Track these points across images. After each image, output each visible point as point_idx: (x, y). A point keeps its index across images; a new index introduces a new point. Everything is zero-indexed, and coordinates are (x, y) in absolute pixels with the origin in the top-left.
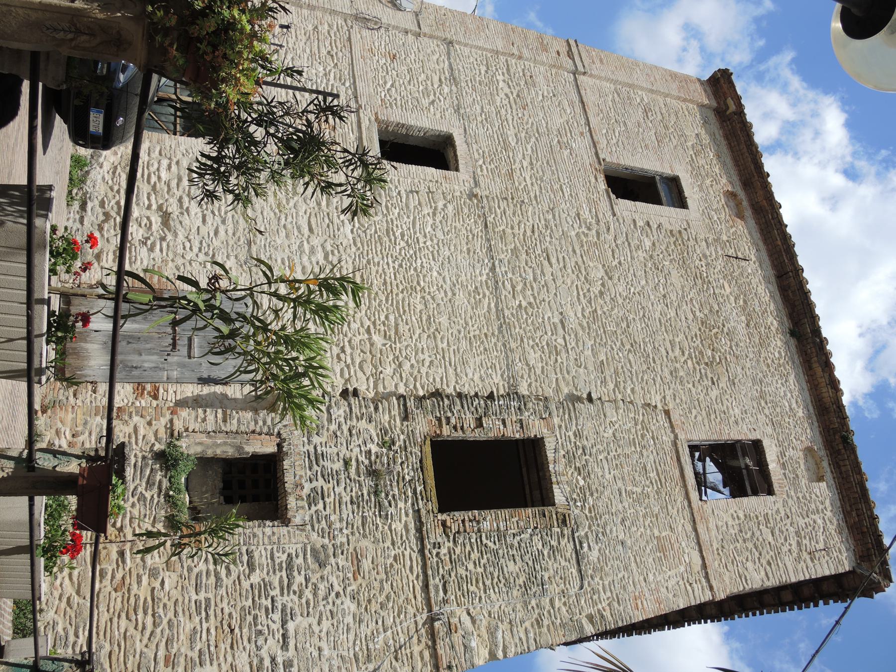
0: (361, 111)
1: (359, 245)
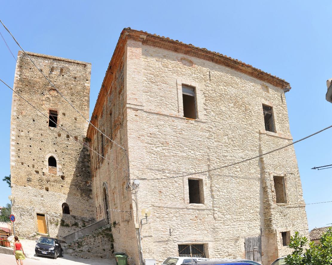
1: (231, 214)
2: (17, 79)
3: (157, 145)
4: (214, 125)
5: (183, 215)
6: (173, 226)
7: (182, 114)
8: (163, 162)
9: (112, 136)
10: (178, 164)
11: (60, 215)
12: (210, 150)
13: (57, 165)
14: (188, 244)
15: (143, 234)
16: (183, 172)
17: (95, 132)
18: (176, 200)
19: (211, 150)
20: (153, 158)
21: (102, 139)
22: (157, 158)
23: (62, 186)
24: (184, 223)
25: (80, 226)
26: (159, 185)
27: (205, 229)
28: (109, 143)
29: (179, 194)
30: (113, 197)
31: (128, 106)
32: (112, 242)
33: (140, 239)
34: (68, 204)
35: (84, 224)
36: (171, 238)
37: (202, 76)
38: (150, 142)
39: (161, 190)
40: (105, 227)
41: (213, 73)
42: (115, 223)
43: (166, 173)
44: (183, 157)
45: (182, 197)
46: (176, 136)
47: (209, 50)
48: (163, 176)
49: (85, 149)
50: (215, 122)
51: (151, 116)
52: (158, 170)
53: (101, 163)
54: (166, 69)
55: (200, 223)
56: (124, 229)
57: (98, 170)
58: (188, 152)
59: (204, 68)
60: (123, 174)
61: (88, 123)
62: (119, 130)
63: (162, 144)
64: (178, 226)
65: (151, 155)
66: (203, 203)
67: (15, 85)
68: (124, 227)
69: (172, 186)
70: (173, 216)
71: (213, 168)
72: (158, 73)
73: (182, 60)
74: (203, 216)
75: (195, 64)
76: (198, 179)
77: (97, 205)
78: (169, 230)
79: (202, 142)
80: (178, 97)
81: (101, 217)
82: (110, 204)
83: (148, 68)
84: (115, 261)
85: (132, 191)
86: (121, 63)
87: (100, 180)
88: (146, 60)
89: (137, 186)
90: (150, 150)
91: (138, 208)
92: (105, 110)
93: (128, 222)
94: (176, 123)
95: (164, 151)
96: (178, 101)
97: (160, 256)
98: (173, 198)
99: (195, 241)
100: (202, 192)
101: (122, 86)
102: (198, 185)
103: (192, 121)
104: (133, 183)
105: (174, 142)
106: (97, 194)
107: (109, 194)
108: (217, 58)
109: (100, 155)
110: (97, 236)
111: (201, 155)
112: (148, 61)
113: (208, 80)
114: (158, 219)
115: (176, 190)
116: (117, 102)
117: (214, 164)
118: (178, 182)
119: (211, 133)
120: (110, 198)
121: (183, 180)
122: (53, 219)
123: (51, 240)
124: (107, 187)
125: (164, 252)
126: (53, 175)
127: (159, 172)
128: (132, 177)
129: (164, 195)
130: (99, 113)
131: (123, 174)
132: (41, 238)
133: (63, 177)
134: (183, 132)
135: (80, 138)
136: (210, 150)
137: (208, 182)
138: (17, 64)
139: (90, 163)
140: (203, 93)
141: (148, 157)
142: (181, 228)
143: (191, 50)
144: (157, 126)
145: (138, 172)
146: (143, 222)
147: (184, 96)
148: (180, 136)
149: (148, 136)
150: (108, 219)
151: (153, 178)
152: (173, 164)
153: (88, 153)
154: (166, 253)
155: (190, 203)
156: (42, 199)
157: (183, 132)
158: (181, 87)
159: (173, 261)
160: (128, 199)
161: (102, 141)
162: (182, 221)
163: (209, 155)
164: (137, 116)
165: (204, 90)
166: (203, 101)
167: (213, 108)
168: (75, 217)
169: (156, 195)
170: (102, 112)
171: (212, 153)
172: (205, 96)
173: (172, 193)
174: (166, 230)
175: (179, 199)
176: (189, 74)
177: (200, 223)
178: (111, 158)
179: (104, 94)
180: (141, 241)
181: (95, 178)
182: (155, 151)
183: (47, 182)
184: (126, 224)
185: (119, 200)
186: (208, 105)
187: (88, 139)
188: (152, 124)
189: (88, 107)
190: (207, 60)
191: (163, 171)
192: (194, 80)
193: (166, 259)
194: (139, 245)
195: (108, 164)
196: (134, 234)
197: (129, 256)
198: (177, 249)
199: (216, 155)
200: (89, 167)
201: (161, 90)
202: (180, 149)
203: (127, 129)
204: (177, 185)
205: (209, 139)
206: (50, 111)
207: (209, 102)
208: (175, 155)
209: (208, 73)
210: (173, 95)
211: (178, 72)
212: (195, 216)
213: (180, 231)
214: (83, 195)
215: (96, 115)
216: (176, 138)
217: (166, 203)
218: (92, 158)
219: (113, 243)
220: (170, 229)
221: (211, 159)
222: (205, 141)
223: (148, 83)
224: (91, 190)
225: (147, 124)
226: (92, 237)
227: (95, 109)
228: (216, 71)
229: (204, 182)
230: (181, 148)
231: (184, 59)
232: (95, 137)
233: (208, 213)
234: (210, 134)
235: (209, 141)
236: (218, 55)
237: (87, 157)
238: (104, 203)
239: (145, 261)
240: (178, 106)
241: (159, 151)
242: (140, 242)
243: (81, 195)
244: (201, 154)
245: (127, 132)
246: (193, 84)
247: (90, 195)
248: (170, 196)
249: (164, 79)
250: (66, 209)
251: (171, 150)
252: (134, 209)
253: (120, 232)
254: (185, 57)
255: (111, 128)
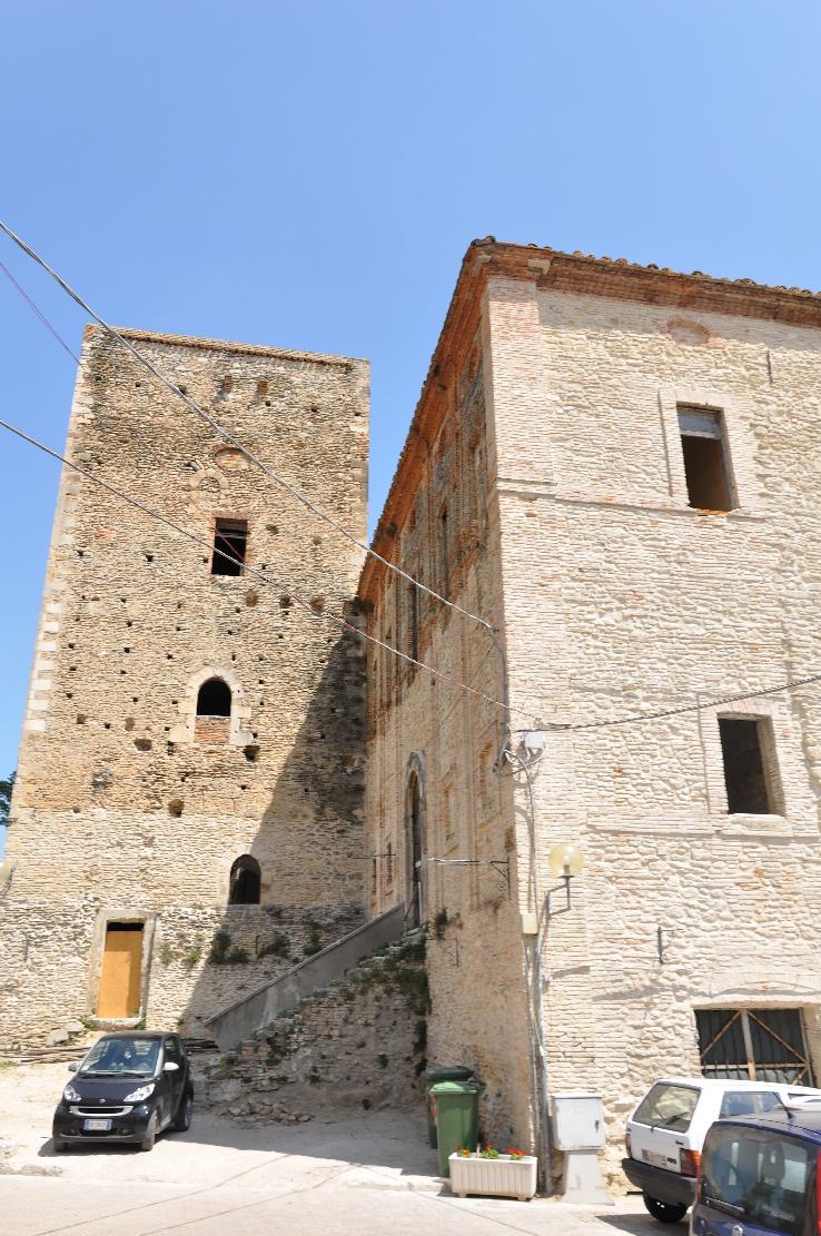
0: (724, 832)
2: (81, 420)
3: (604, 606)
4: (797, 526)
5: (708, 863)
6: (673, 917)
7: (682, 498)
8: (627, 663)
9: (447, 585)
10: (680, 664)
11: (214, 912)
12: (788, 612)
13: (234, 708)
14: (733, 1007)
15: (553, 960)
16: (699, 694)
17: (387, 579)
18: (677, 801)
19: (793, 609)
20: (591, 651)
21: (414, 600)
22: (604, 648)
23: (243, 787)
24: (712, 902)
25: (296, 951)
26: (613, 744)
27: (801, 931)
28: (438, 610)
29: (689, 777)
30: (443, 805)
31: (501, 486)
32: (422, 1013)
33: (541, 985)
34: (260, 857)
35: (315, 939)
36: (666, 974)
37: (743, 371)
38: (579, 597)
39: (621, 766)
40: (401, 944)
41: (780, 356)
42: (442, 920)
43: (636, 697)
44: (694, 639)
45: (699, 789)
46: (668, 572)
47: (760, 282)
48: (629, 712)
49: (350, 640)
50: (799, 514)
51: (582, 513)
52: (612, 692)
53: (405, 684)
54: (623, 361)
55: (778, 900)
56: (478, 943)
57: (394, 709)
58: (713, 622)
59: (747, 345)
60: (484, 713)
61: (365, 553)
62: (472, 570)
63: (622, 601)
64: (689, 916)
65: (584, 640)
66: (782, 814)
67: (70, 441)
68: (479, 932)
69: (662, 747)
70: (668, 867)
71: (805, 672)
72: (595, 376)
73: (672, 326)
74: (786, 868)
75: (717, 335)
76: (754, 719)
77: (378, 848)
78: (654, 936)
79: (757, 584)
80: (665, 447)
81: (386, 899)
82: (432, 841)
83: (561, 362)
84: (425, 1121)
85: (515, 776)
86: (473, 356)
87: (399, 745)
88: (554, 338)
89: (536, 756)
90: (583, 624)
91: (536, 844)
92: (425, 505)
93: (496, 907)
94: (664, 530)
95: (630, 624)
96: (666, 458)
97: (622, 1075)
98: (666, 791)
99: (764, 992)
100: (771, 767)
101: (480, 424)
102: (756, 741)
103: (719, 519)
104: (522, 744)
105: (661, 592)
106: (382, 799)
107: (429, 797)
108: (793, 305)
109: (405, 657)
110: (363, 992)
111: (758, 629)
112: (561, 343)
113: (763, 382)
114: (612, 887)
115: (675, 760)
116: (466, 478)
117: (808, 659)
118: (681, 732)
119: (786, 553)
120: (430, 814)
121: (699, 722)
122: (181, 936)
123: (143, 1047)
124: (423, 768)
125: (638, 1051)
126: (213, 747)
127: (613, 698)
128: (517, 722)
129: (635, 782)
130: (403, 515)
131: (486, 715)
132: (103, 1044)
133: (251, 753)
134: (691, 557)
135: (331, 604)
136: (788, 612)
137: (790, 724)
138: (83, 369)
139: (364, 685)
140: (751, 425)
141: (574, 649)
142: (703, 924)
143: (699, 292)
144: (603, 545)
145: (538, 702)
146: (555, 904)
147: (689, 444)
148: (680, 569)
149: (573, 579)
150: (416, 902)
151: (591, 718)
152: (660, 665)
153: (360, 653)
154: (648, 1057)
155: (731, 812)
156: (148, 852)
157: (691, 557)
158: (674, 413)
159: (677, 1102)
160: (498, 809)
161: (414, 608)
162: (706, 891)
163: (787, 626)
164: (534, 516)
165: (752, 415)
166: (752, 450)
167: (788, 469)
168: (276, 913)
169: (606, 784)
170: (414, 513)
171: (798, 621)
172: (758, 435)
173: (663, 774)
174: (644, 937)
175: (688, 798)
176: (698, 371)
177: (778, 900)
178: (444, 662)
179: (417, 457)
180: (543, 997)
181: (378, 741)
182: (596, 626)
183: (183, 780)
184: (485, 919)
185: (464, 817)
186: (768, 461)
187: (361, 606)
188: (586, 539)
189: (365, 497)
190: (755, 316)
191: (627, 693)
192: (715, 387)
193: (646, 1090)
194: (533, 1016)
195: (433, 684)
196: (516, 969)
197: (488, 1082)
198: (690, 1032)
199: (812, 628)
200: (359, 701)
201: (608, 428)
202: (684, 613)
203: (500, 561)
204: (679, 741)
205: (779, 571)
206: (219, 520)
207: (771, 454)
208: (667, 633)
209: (762, 360)
210: (650, 442)
211: (662, 366)
212: (752, 870)
213: (699, 941)
214: (328, 811)
215: (393, 525)
216: (667, 576)
217: (639, 817)
218: (375, 669)
219: (427, 1018)
220: (659, 932)
221: (796, 643)
222: (768, 579)
223: (567, 411)
224: (360, 790)
225: (567, 540)
226: (341, 999)
227: (387, 507)
228: (788, 348)
229: (775, 725)
230: (685, 609)
231: (680, 324)
232: (389, 594)
233: (804, 855)
234: (783, 556)
235: (782, 579)
236: (795, 297)
237: (353, 667)
238: (407, 835)
239: (555, 1110)
240: (669, 476)
241: (613, 626)
242: (537, 1003)
243: (320, 812)
244: (759, 625)
245: (500, 568)
246: (714, 401)
247: (356, 808)
248: (657, 787)
249: (617, 393)
250: (246, 881)
251: (652, 617)
252: (523, 848)
253: (462, 958)
254: (684, 318)
255: (445, 562)
